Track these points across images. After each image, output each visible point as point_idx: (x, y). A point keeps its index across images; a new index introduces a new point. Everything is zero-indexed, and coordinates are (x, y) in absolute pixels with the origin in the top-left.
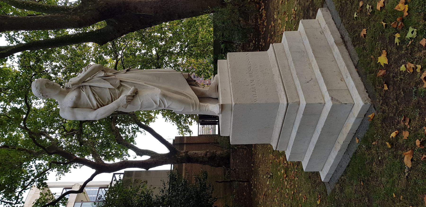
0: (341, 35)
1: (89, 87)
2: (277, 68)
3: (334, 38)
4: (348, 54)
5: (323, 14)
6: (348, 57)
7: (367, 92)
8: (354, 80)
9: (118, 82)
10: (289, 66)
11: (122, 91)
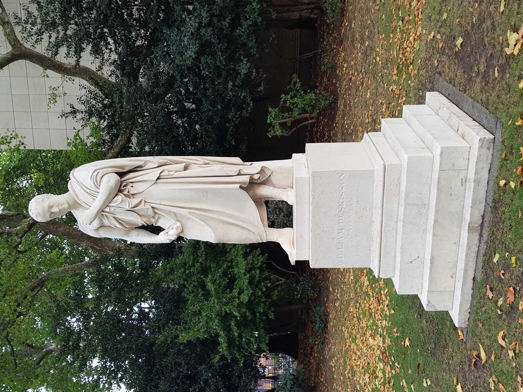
0: (485, 211)
1: (112, 218)
2: (380, 219)
3: (471, 215)
4: (476, 249)
5: (479, 156)
6: (474, 255)
7: (469, 313)
8: (463, 295)
9: (150, 212)
10: (398, 214)
11: (159, 218)
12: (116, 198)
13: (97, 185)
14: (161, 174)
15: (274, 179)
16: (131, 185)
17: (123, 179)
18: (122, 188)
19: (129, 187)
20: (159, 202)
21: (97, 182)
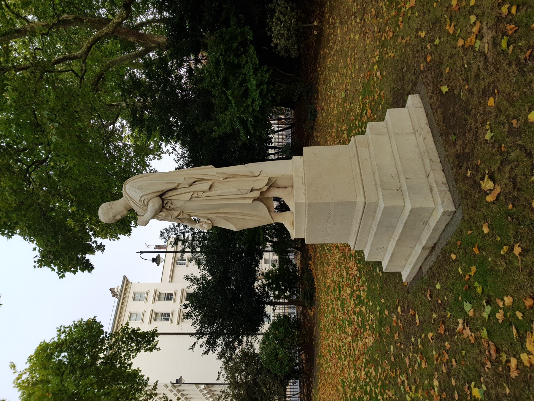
12: (161, 213)
15: (280, 183)
17: (163, 197)
19: (169, 204)
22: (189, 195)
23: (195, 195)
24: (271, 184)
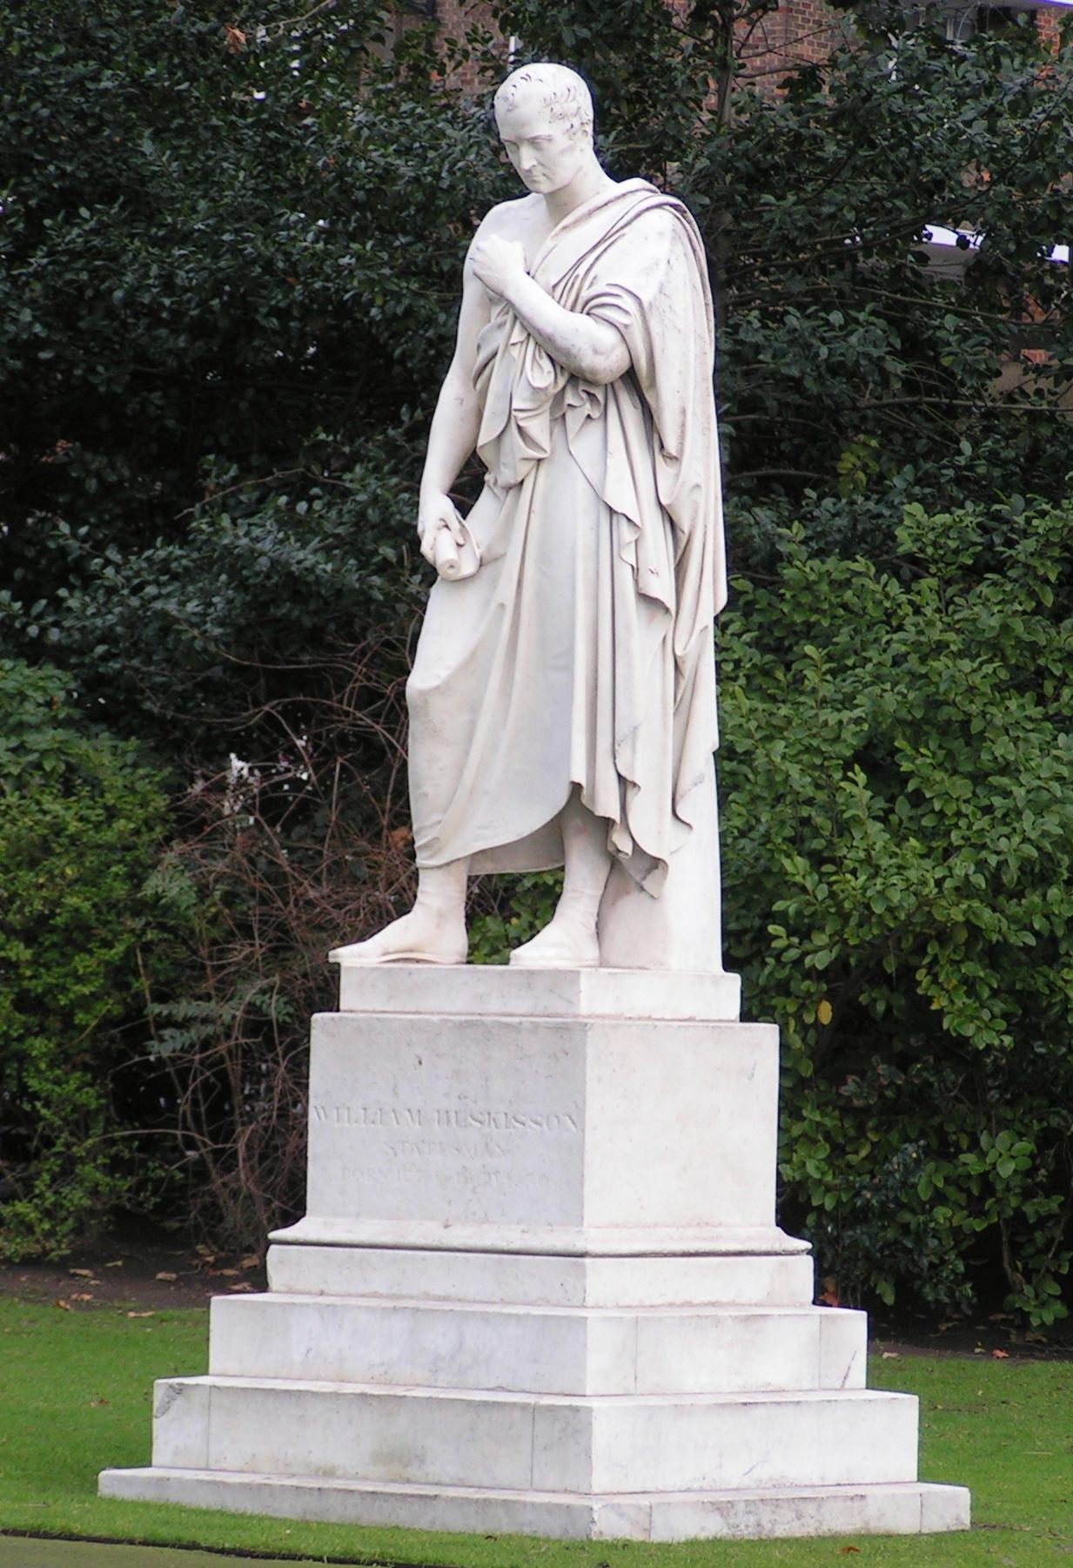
13: (587, 307)
14: (624, 521)
15: (630, 908)
16: (596, 414)
18: (582, 387)
19: (587, 408)
20: (536, 506)
21: (603, 305)
22: (624, 504)
23: (627, 535)
24: (630, 872)
